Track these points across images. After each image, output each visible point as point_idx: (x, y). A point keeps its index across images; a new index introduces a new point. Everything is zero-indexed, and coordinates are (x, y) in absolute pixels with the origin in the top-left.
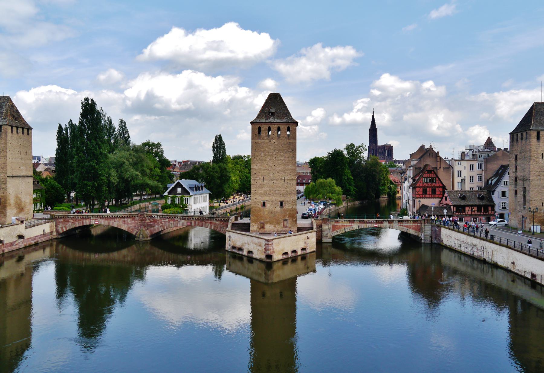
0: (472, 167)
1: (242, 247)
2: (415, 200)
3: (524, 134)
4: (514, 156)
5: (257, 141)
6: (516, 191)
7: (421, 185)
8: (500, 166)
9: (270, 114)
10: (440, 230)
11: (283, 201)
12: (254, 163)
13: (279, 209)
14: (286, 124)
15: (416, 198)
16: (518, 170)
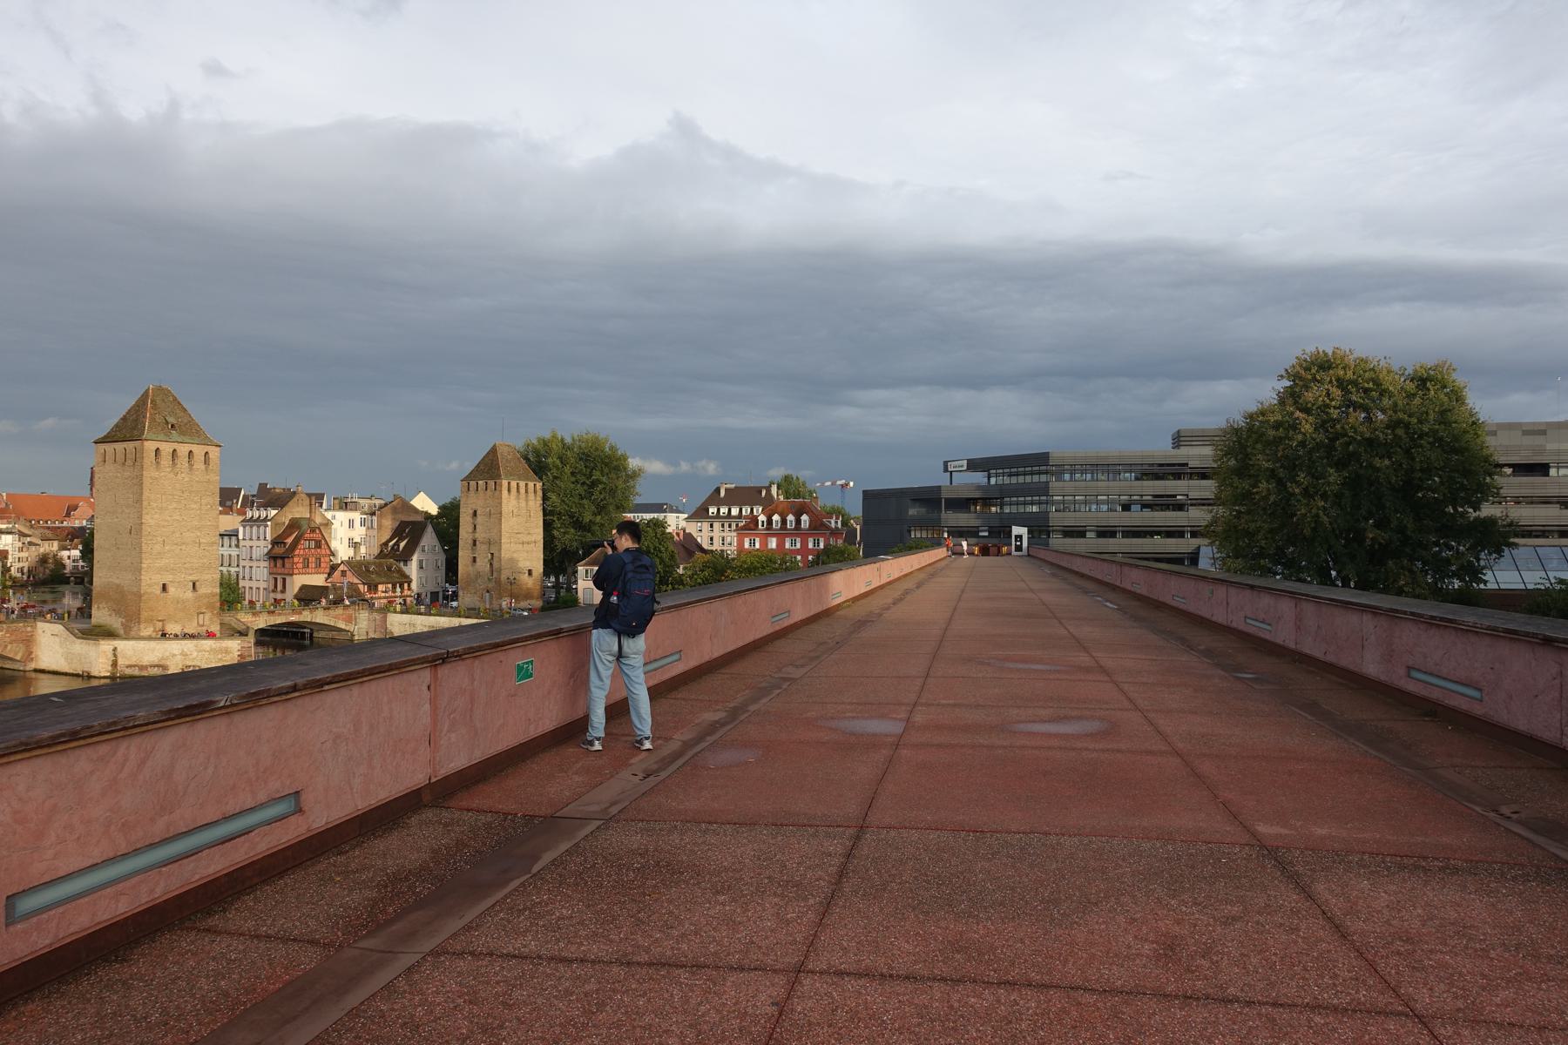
0: (351, 523)
1: (161, 663)
2: (284, 580)
3: (491, 483)
4: (471, 512)
5: (153, 474)
6: (475, 557)
7: (302, 552)
8: (398, 523)
9: (170, 427)
10: (385, 618)
11: (198, 581)
12: (147, 514)
13: (189, 594)
14: (203, 446)
15: (292, 575)
16: (478, 530)
